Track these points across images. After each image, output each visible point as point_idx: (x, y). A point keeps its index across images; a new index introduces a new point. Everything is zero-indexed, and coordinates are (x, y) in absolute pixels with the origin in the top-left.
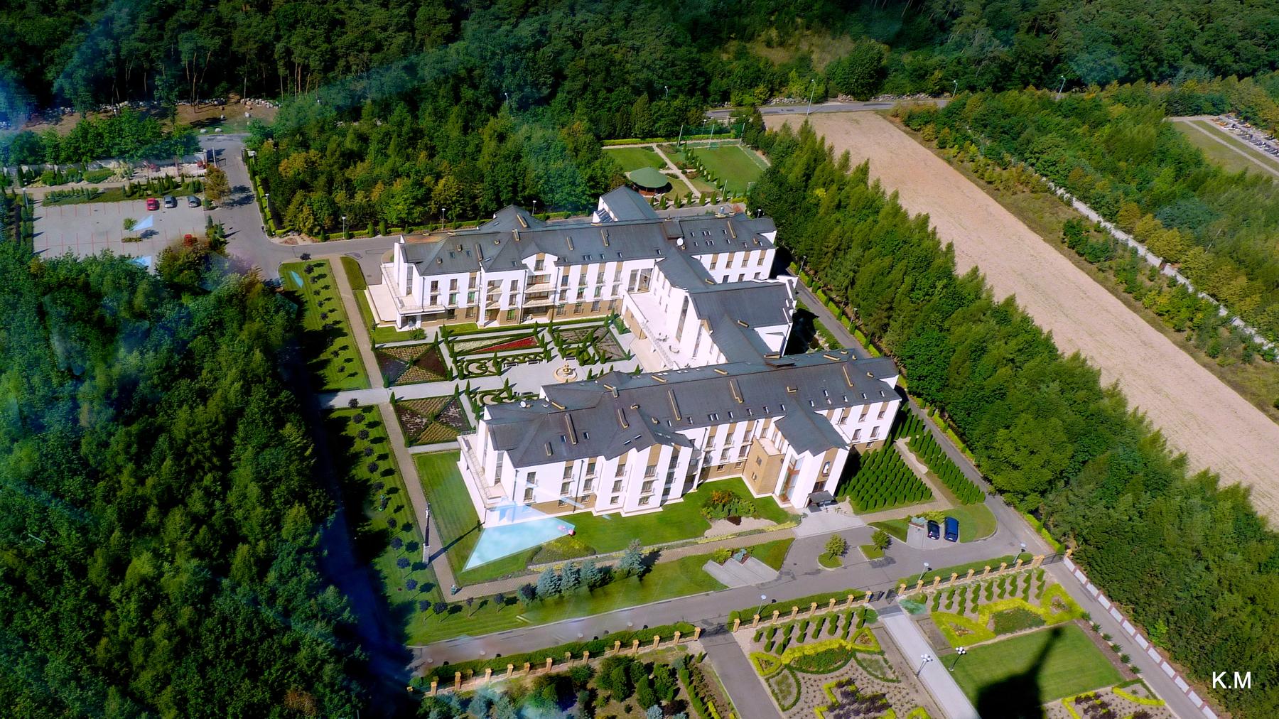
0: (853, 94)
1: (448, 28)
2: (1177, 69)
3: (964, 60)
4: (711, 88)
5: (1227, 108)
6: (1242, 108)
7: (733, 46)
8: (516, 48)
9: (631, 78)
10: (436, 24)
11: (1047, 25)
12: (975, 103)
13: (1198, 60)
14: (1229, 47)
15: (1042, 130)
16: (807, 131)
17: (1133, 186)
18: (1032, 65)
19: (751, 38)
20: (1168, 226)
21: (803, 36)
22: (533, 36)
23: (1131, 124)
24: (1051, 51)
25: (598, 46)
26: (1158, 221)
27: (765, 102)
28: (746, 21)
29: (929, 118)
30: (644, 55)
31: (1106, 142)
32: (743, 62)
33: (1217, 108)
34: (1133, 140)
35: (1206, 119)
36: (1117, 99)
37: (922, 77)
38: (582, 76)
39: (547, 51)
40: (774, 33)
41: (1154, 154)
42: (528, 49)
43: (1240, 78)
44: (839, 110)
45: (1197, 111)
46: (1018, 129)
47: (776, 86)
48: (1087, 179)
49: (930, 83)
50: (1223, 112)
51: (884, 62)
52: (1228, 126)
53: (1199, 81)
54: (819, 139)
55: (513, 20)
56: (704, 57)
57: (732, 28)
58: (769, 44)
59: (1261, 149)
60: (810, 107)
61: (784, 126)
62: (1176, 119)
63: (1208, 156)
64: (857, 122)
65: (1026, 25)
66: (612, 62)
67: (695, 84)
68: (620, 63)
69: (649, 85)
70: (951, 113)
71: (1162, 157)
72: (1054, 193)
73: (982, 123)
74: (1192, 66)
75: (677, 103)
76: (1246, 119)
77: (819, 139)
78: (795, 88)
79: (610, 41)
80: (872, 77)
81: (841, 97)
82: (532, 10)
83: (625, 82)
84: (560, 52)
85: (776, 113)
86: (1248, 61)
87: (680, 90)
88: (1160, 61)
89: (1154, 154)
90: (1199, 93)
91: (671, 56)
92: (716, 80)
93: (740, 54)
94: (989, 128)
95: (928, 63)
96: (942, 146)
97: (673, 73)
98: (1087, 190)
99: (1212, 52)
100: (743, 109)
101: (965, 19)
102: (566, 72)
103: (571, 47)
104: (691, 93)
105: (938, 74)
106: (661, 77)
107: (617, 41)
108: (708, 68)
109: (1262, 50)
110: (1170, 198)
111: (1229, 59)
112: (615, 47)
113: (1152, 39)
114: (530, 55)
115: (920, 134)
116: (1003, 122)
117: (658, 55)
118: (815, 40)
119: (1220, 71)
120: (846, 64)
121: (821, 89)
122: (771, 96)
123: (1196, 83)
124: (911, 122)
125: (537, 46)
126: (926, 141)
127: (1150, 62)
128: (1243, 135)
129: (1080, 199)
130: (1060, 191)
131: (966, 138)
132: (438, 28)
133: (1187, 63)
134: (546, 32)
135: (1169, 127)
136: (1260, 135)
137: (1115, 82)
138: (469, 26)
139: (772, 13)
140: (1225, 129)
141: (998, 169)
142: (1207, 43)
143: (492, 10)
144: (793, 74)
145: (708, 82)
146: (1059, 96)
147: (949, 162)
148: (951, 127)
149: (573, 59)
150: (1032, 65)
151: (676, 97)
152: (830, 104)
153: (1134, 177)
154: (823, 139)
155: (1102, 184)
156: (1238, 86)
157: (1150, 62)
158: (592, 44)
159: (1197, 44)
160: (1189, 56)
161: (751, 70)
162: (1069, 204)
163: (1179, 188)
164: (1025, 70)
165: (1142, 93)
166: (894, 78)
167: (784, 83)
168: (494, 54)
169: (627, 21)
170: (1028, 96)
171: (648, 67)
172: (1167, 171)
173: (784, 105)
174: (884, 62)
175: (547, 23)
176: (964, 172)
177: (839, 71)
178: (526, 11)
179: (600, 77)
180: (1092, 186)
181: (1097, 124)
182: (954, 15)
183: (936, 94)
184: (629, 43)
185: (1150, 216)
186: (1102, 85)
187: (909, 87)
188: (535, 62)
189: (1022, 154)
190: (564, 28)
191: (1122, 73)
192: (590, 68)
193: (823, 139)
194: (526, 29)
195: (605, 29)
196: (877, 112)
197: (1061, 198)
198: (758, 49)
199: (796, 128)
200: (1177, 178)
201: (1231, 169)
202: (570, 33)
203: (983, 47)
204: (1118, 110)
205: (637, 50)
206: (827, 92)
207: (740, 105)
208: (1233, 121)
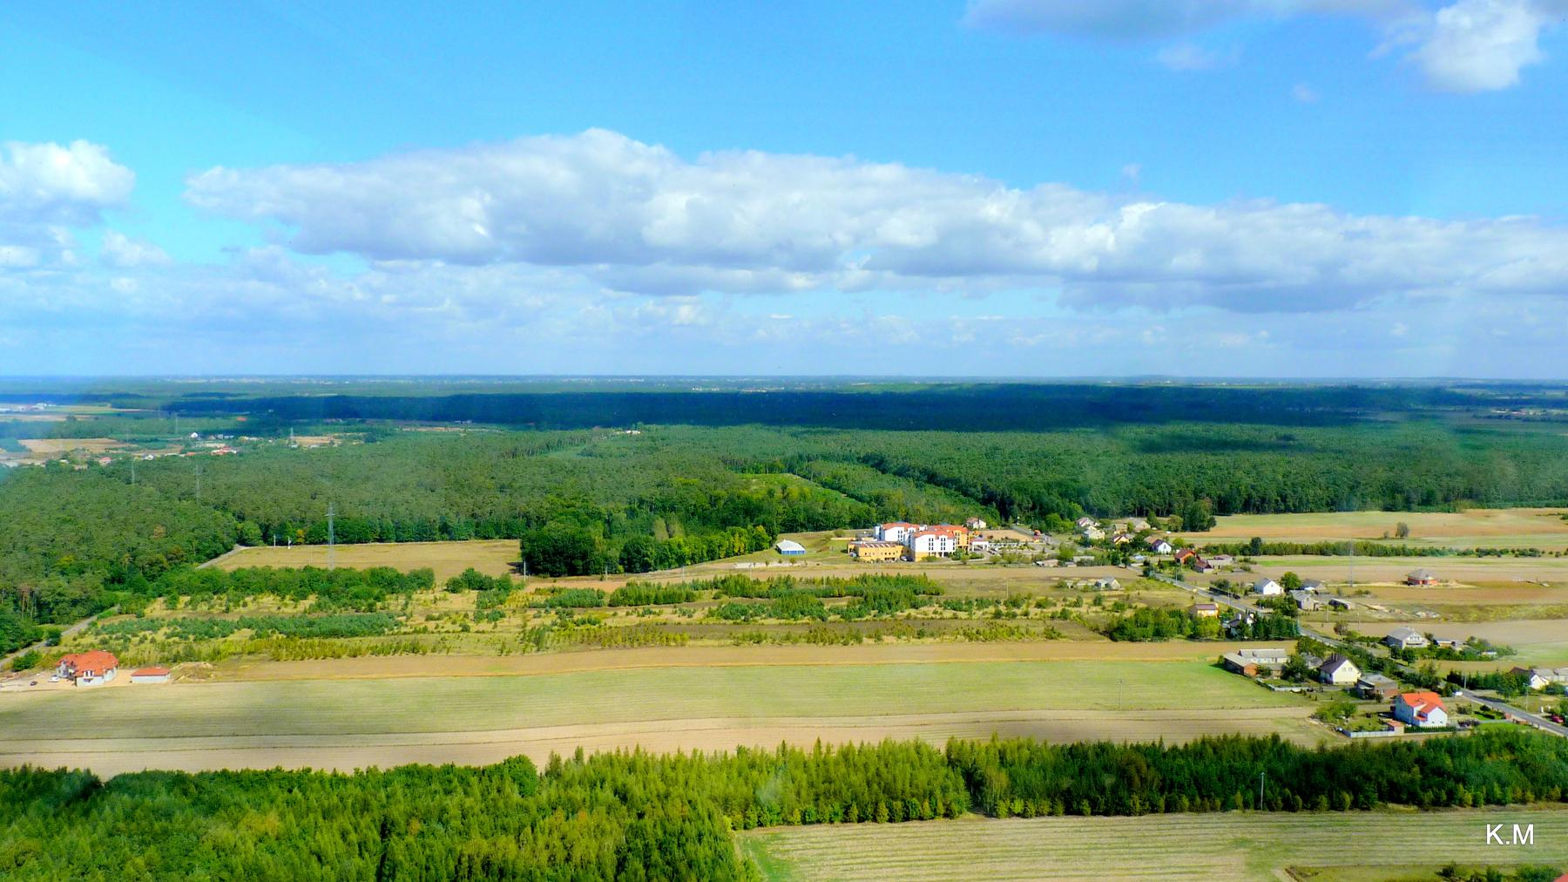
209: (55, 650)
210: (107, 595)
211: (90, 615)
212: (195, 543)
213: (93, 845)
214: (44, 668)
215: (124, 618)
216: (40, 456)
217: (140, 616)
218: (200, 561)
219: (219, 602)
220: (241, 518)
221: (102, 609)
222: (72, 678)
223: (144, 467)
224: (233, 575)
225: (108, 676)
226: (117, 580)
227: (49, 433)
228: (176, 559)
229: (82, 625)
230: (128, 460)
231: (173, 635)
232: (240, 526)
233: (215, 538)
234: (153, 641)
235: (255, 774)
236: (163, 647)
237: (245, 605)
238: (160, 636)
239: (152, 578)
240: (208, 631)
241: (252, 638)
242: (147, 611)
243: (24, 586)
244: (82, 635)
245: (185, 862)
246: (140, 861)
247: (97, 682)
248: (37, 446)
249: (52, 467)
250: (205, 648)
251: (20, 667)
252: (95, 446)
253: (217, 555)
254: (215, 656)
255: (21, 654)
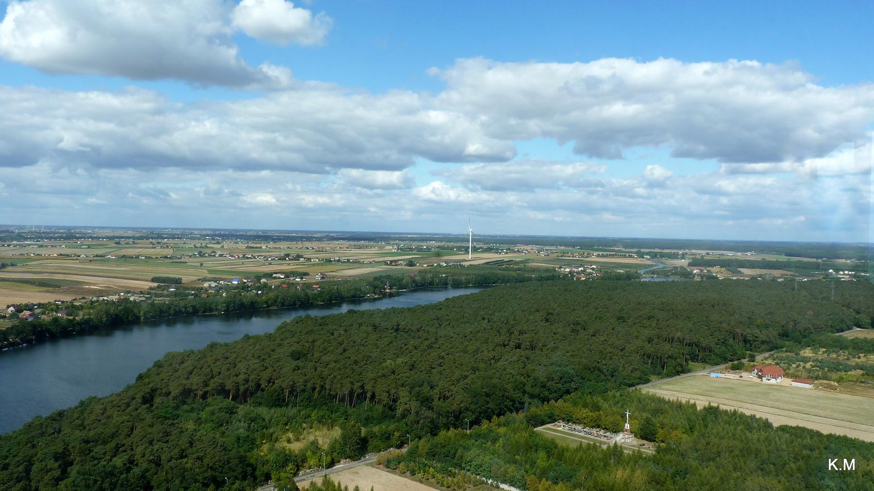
0: (350, 457)
1: (57, 473)
2: (523, 403)
3: (409, 423)
4: (257, 473)
5: (557, 418)
6: (563, 416)
7: (265, 447)
8: (112, 474)
9: (200, 478)
10: (48, 471)
11: (448, 394)
12: (424, 444)
13: (532, 396)
14: (544, 386)
15: (467, 449)
16: (327, 482)
17: (528, 466)
18: (448, 417)
19: (277, 440)
20: (556, 483)
21: (309, 433)
22: (125, 464)
23: (513, 434)
24: (454, 407)
25: (174, 461)
26: (549, 482)
27: (295, 474)
28: (271, 430)
29: (399, 460)
30: (206, 461)
31: (503, 447)
32: (274, 453)
33: (552, 419)
34: (517, 442)
35: (549, 426)
36: (499, 425)
37: (388, 438)
38: (164, 484)
39: (136, 471)
40: (290, 435)
41: (531, 448)
42: (121, 474)
43: (556, 401)
44: (344, 469)
45: (543, 423)
46: (452, 452)
47: (299, 463)
48: (502, 469)
49: (394, 440)
50: (555, 421)
51: (363, 435)
52: (561, 427)
53: (537, 407)
54: (336, 485)
55: (108, 457)
56: (248, 454)
57: (263, 436)
58: (289, 441)
59: (582, 434)
60: (325, 472)
61: (312, 483)
62: (535, 429)
63: (560, 443)
64: (357, 473)
65: (438, 396)
66: (185, 470)
67: (245, 472)
68: (191, 469)
69: (214, 480)
70: (412, 454)
71: (536, 448)
72: (487, 483)
73: (432, 454)
74: (530, 400)
75: (236, 486)
76: (568, 421)
77: (336, 485)
78: (312, 462)
79: (182, 457)
80: (358, 444)
81: (342, 461)
82: (121, 449)
83: (196, 481)
84: (147, 470)
85: (304, 480)
86: (556, 392)
87: (236, 478)
88: (513, 401)
89: (531, 448)
90: (539, 413)
91: (226, 457)
92: (259, 466)
93: (271, 450)
94: (436, 457)
95: (389, 429)
96: (413, 473)
97: (230, 468)
98: (505, 476)
99: (537, 391)
100: (282, 482)
101: (402, 400)
102: (153, 483)
103: (153, 465)
104: (244, 478)
105: (397, 434)
106: (221, 472)
107: (186, 456)
108: (252, 461)
109: (560, 386)
110: (550, 467)
111: (546, 393)
112: (185, 460)
113: (505, 390)
114: (124, 476)
115: (397, 471)
116: (444, 450)
117: (217, 458)
118: (317, 433)
119: (545, 400)
120: (341, 440)
121: (329, 459)
122: (298, 470)
123: (536, 409)
124: (390, 465)
125: (128, 470)
126: (403, 474)
127: (508, 403)
128: (570, 429)
129: (502, 482)
130: (490, 482)
131: (425, 465)
132: (49, 474)
133: (526, 399)
134: (134, 461)
135: (534, 432)
136: (579, 427)
137: (495, 417)
138: (74, 470)
139: (286, 424)
140: (560, 429)
141: (450, 478)
142: (532, 386)
143: (91, 454)
144: (309, 453)
145: (254, 469)
146: (468, 432)
147: (421, 482)
148: (414, 461)
149: (156, 474)
150: (448, 417)
151: (233, 484)
152: (337, 466)
153: (526, 462)
154: (339, 483)
155: (511, 469)
156: (557, 405)
157: (508, 403)
158: (169, 461)
159: (527, 388)
160: (526, 395)
161: (281, 456)
162: (498, 487)
163: (552, 461)
164: (444, 420)
165: (511, 419)
166: (372, 443)
167: (304, 460)
168: (95, 481)
169: (191, 444)
170: (452, 432)
171: (211, 468)
172: (542, 454)
173: (308, 474)
174: (363, 435)
175: (133, 455)
176: (431, 485)
177: (338, 446)
178: (117, 450)
179: (177, 482)
180: (506, 472)
181: (495, 441)
182: (395, 401)
183: (400, 447)
184: (195, 456)
185: (544, 480)
186: (489, 419)
187: (382, 446)
188: (128, 481)
189: (460, 466)
190: (147, 455)
191: (496, 412)
192: (170, 476)
193: (339, 483)
194: (118, 461)
195: (177, 450)
196: (367, 465)
197: (492, 485)
198: (282, 444)
199: (319, 481)
200: (548, 457)
201: (573, 446)
202: (151, 458)
203: (417, 413)
204: (502, 430)
205: (200, 458)
206: (333, 459)
207: (279, 480)
208: (562, 424)
209: (752, 363)
210: (780, 342)
211: (770, 350)
212: (830, 323)
213: (768, 452)
214: (746, 371)
215: (788, 354)
216: (747, 276)
217: (797, 354)
218: (832, 332)
219: (843, 356)
220: (858, 313)
221: (777, 348)
222: (760, 377)
223: (802, 285)
224: (852, 341)
225: (779, 380)
226: (785, 335)
227: (752, 265)
228: (818, 329)
229: (767, 355)
230: (792, 280)
231: (815, 366)
232: (857, 316)
233: (842, 321)
234: (804, 367)
235: (864, 442)
236: (809, 371)
237: (859, 358)
238: (808, 366)
239: (805, 337)
240: (836, 367)
241: (863, 375)
242: (802, 353)
243: (739, 331)
244: (766, 359)
245: (820, 474)
246: (793, 465)
247: (773, 381)
248: (747, 272)
249: (753, 278)
250: (834, 376)
251: (735, 368)
252: (776, 273)
253: (842, 331)
254: (840, 380)
255: (736, 362)
